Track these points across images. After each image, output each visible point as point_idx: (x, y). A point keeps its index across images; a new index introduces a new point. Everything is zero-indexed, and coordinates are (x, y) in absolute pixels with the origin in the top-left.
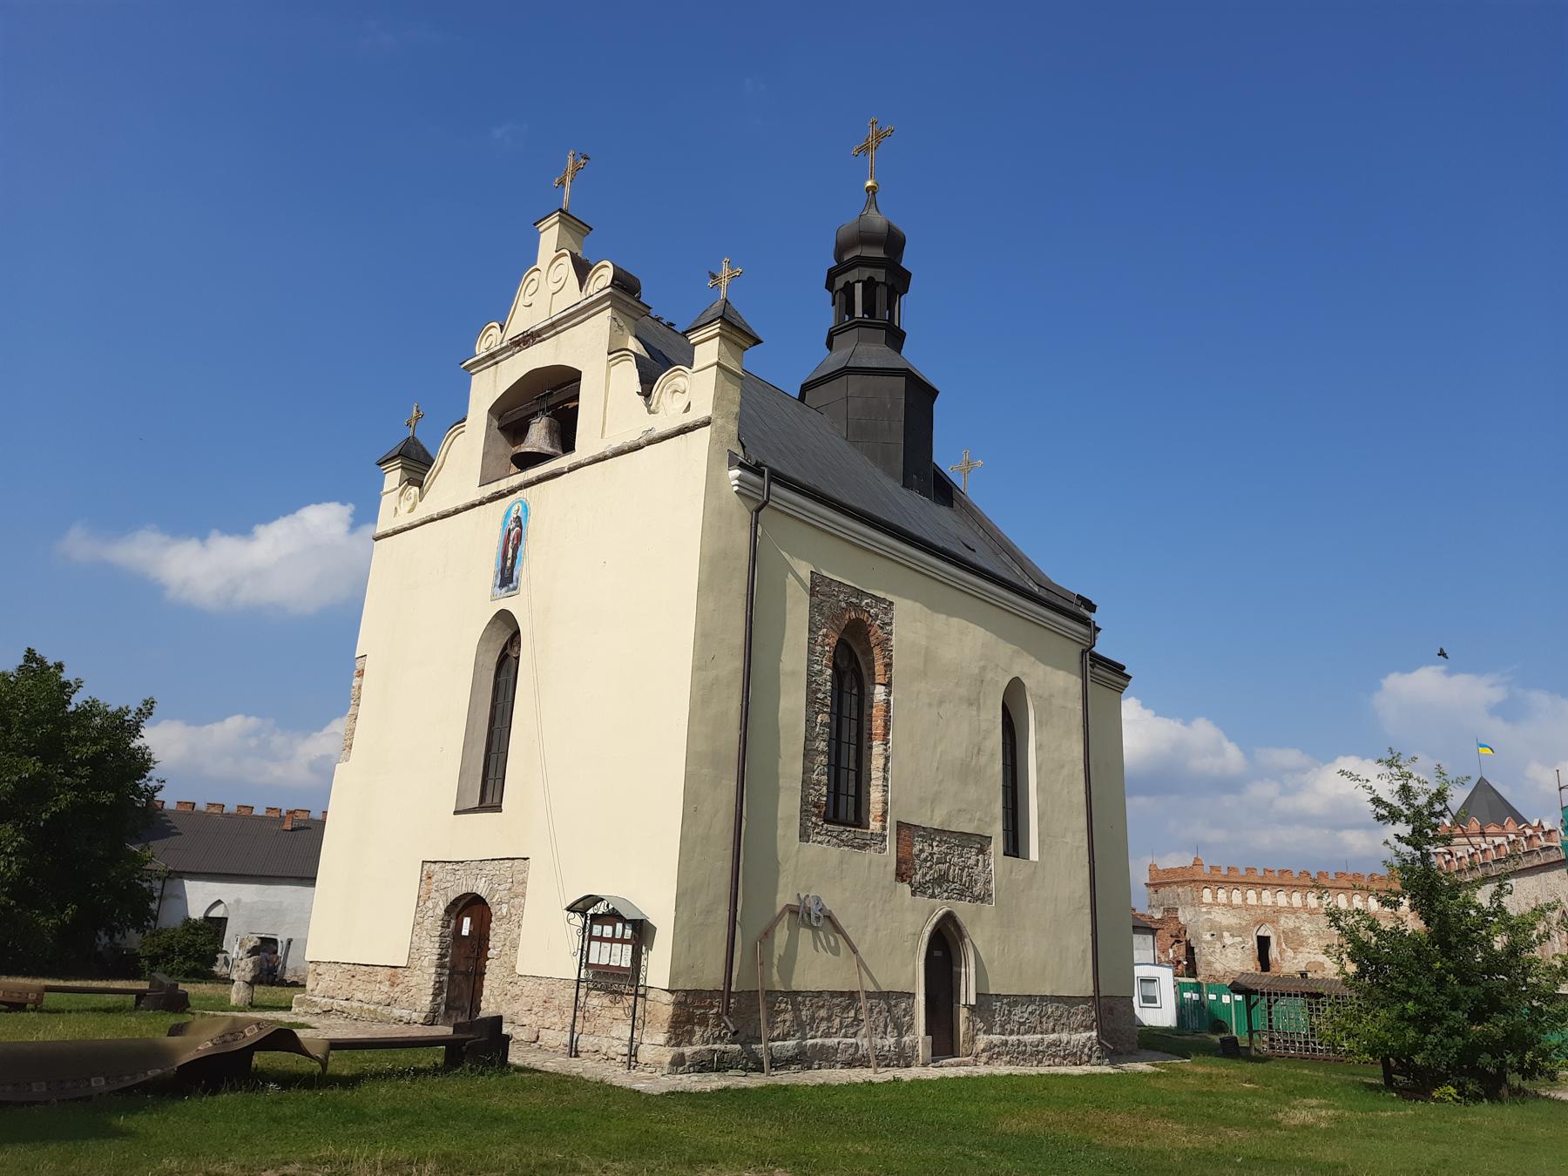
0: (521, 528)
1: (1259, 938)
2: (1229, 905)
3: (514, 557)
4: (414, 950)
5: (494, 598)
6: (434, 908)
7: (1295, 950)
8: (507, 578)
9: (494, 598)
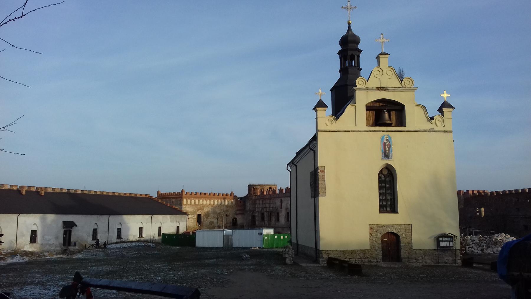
1: (198, 215)
4: (372, 246)
5: (382, 159)
8: (386, 155)
9: (382, 159)
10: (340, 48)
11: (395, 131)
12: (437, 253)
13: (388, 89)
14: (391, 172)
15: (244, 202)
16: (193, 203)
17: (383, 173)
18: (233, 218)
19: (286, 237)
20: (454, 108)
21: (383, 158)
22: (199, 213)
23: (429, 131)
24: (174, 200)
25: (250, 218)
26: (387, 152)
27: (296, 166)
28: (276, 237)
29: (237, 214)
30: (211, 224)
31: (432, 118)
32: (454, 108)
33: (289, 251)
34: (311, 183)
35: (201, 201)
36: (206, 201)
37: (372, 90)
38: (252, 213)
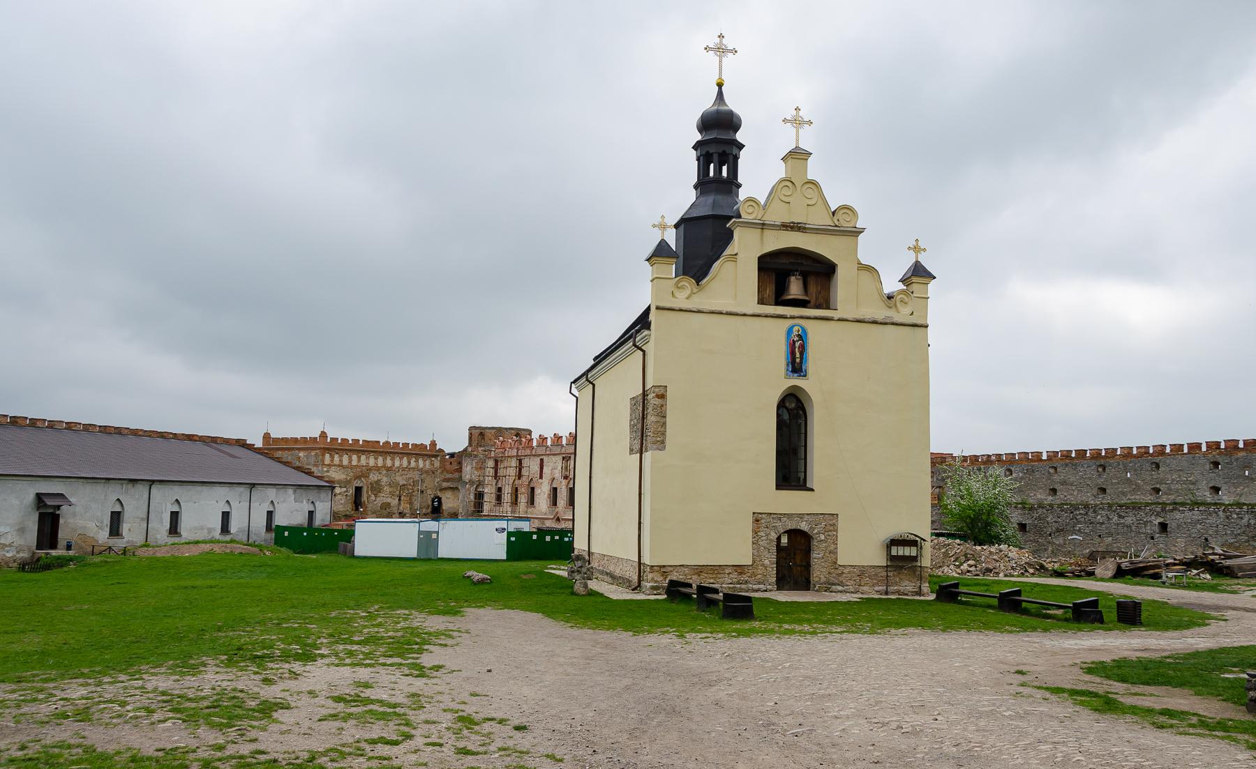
0: (803, 341)
1: (356, 487)
2: (339, 466)
3: (802, 358)
7: (376, 496)
8: (796, 367)
10: (699, 137)
11: (816, 318)
12: (885, 574)
13: (805, 228)
14: (802, 404)
15: (460, 463)
16: (345, 462)
17: (787, 405)
18: (432, 496)
19: (557, 538)
20: (935, 278)
21: (792, 374)
23: (882, 321)
24: (301, 454)
25: (472, 497)
26: (798, 360)
27: (594, 385)
28: (535, 537)
29: (441, 490)
30: (385, 509)
31: (890, 297)
32: (935, 278)
33: (581, 567)
34: (631, 420)
35: (363, 457)
36: (376, 459)
37: (773, 227)
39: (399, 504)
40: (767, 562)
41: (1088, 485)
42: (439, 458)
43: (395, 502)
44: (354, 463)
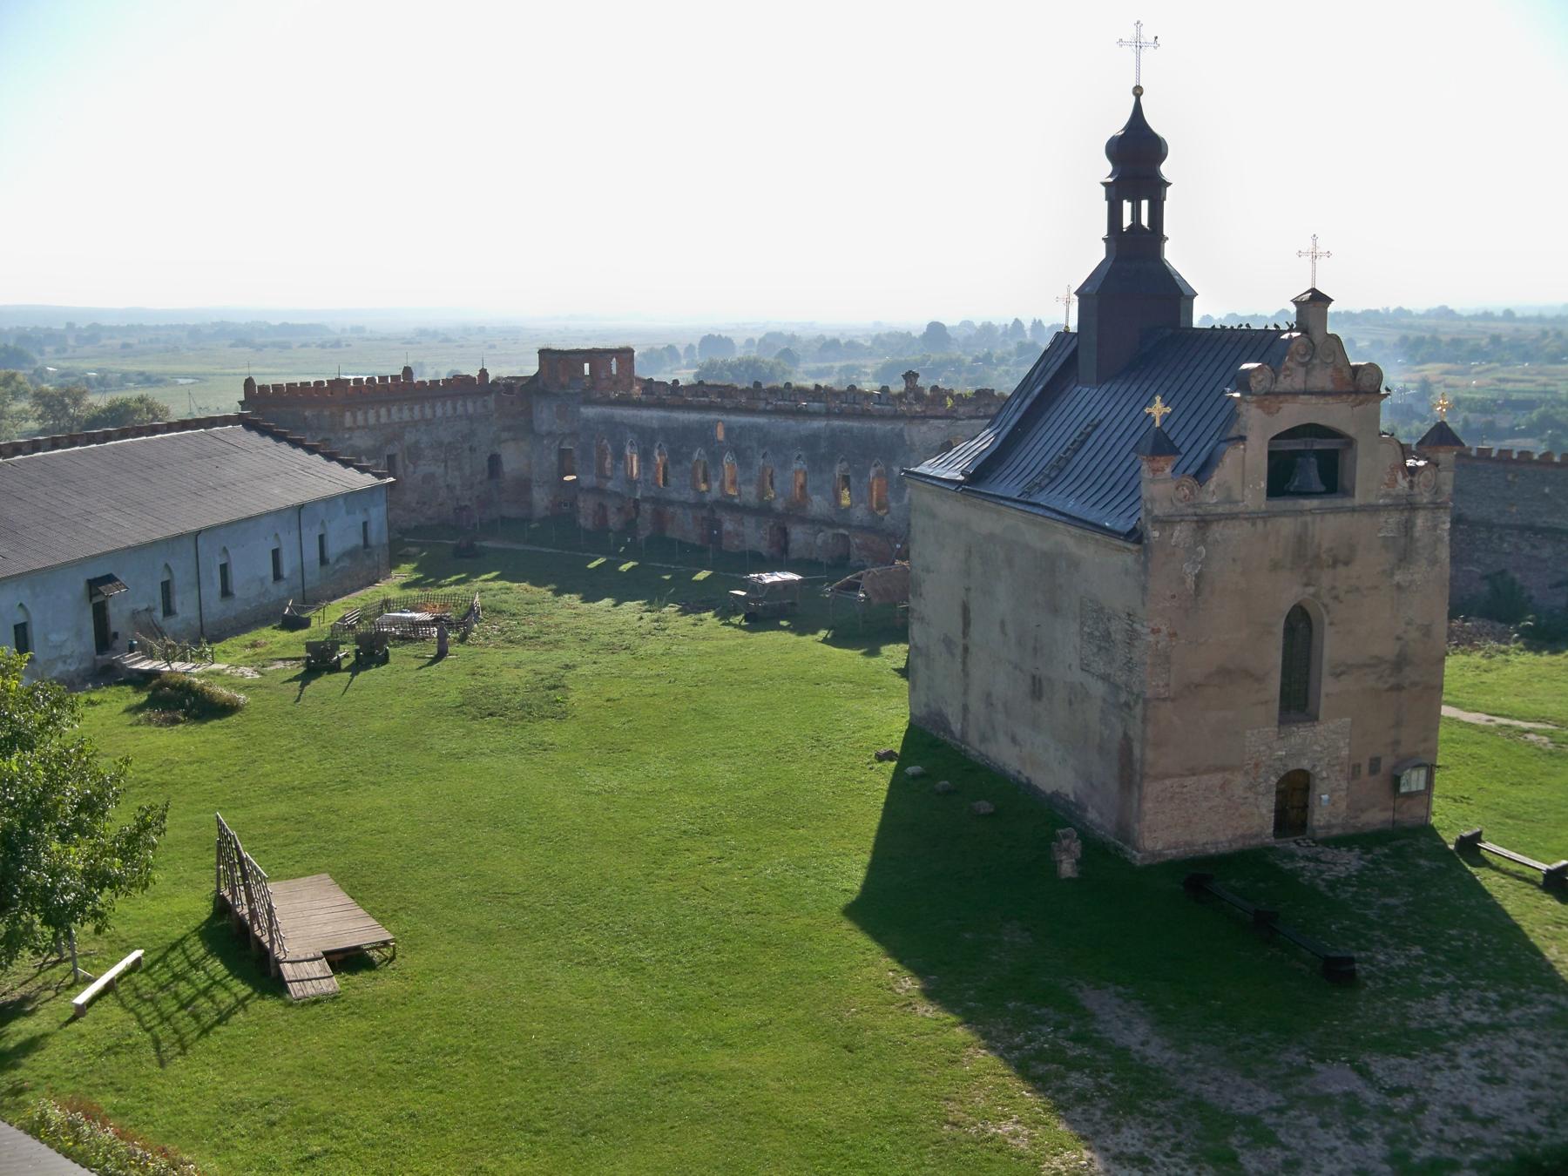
1: (389, 457)
2: (364, 427)
6: (1265, 781)
16: (372, 421)
18: (488, 455)
22: (389, 450)
25: (554, 458)
35: (394, 410)
36: (411, 410)
38: (561, 443)
39: (447, 473)
40: (1264, 811)
41: (1492, 497)
42: (493, 396)
43: (439, 470)
44: (383, 420)
